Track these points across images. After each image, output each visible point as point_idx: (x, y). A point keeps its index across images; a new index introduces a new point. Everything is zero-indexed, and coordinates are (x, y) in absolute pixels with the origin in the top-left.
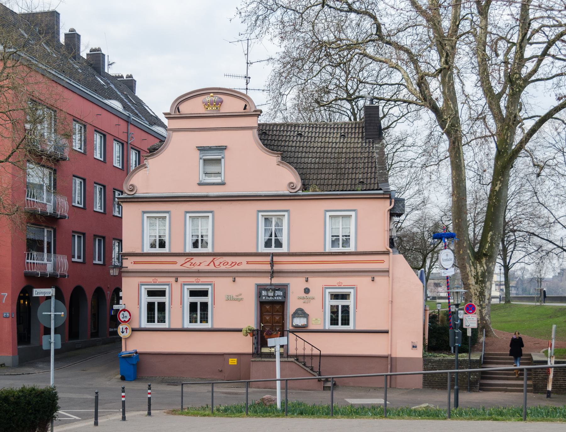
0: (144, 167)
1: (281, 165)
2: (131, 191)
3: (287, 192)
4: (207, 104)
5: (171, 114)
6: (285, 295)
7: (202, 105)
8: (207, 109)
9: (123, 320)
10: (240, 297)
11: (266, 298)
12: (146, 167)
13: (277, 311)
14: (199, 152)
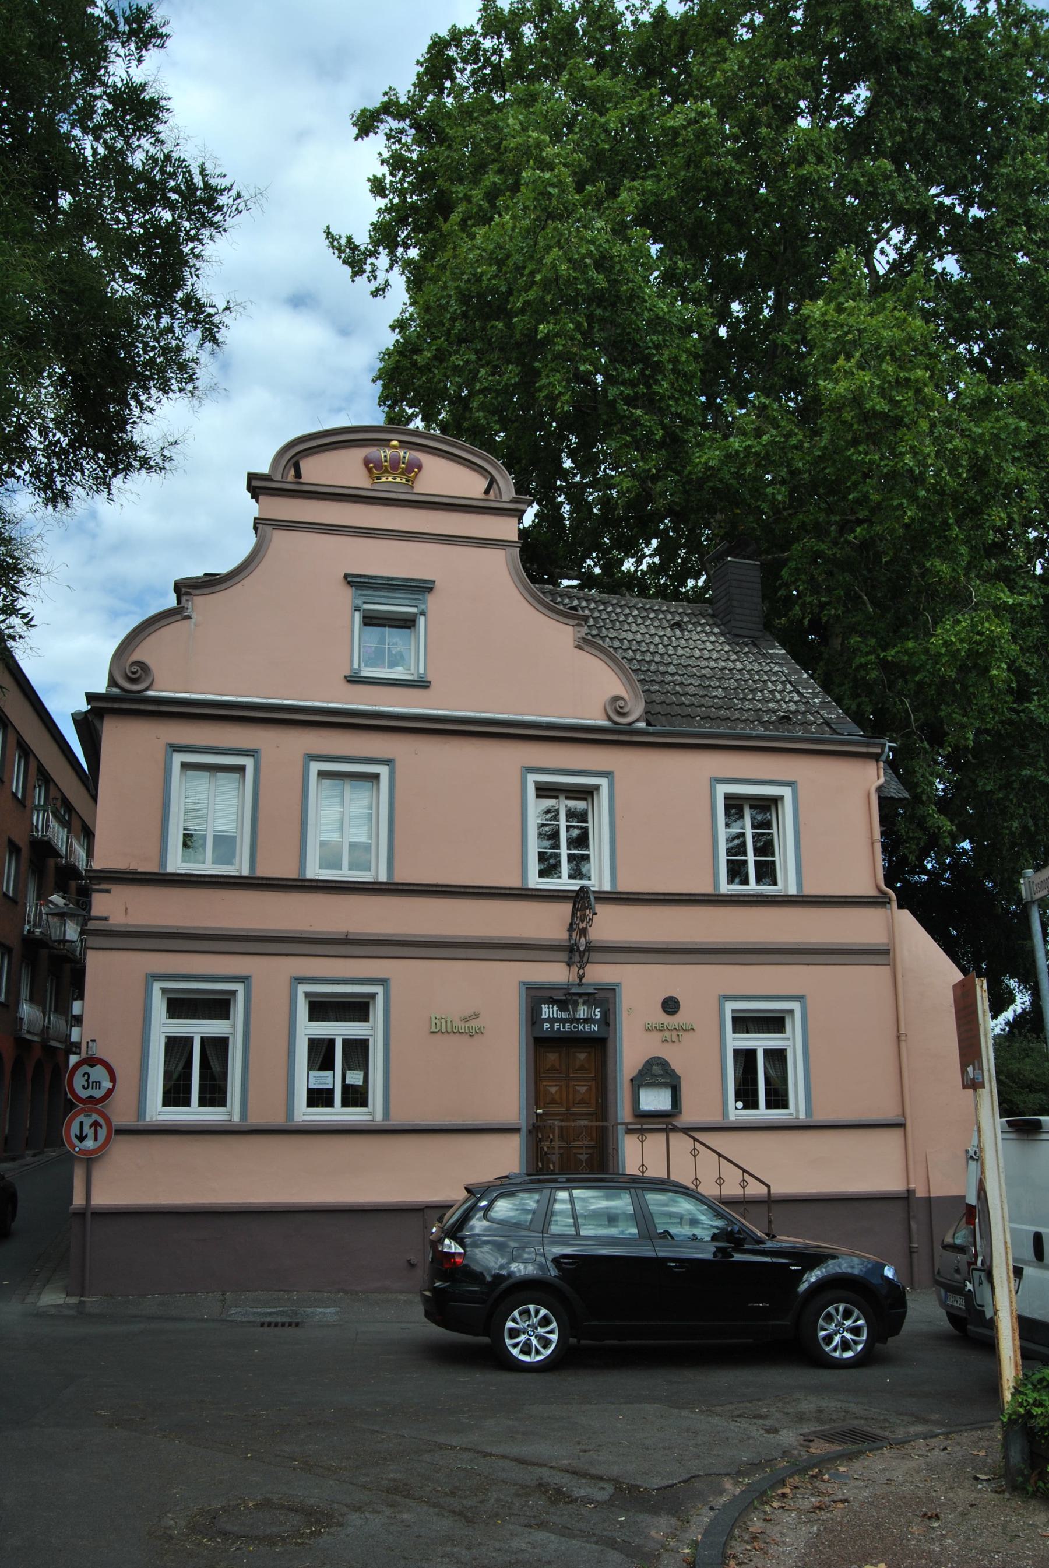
0: (179, 617)
1: (586, 647)
2: (133, 681)
3: (603, 723)
4: (372, 467)
5: (271, 480)
6: (607, 1021)
7: (364, 471)
8: (379, 478)
9: (84, 1094)
10: (474, 1024)
11: (552, 1027)
12: (189, 617)
13: (582, 1068)
14: (348, 592)
